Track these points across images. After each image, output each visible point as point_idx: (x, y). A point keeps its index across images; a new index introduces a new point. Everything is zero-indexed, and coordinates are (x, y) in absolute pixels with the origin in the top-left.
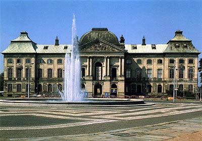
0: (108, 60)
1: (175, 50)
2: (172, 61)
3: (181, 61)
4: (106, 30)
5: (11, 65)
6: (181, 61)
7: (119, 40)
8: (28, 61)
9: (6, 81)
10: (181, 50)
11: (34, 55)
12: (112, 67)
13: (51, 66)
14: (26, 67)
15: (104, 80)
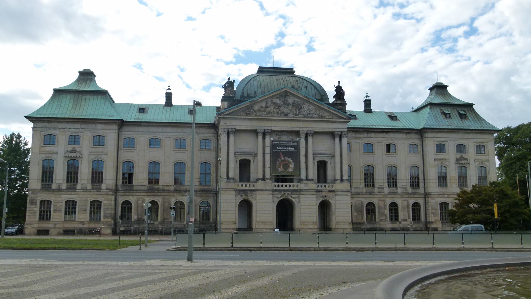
0: (310, 139)
1: (445, 123)
2: (441, 148)
3: (461, 148)
4: (290, 72)
5: (49, 148)
6: (461, 148)
7: (331, 92)
8: (99, 140)
9: (34, 191)
10: (456, 123)
11: (115, 127)
12: (318, 159)
13: (155, 155)
14: (93, 157)
15: (301, 191)
